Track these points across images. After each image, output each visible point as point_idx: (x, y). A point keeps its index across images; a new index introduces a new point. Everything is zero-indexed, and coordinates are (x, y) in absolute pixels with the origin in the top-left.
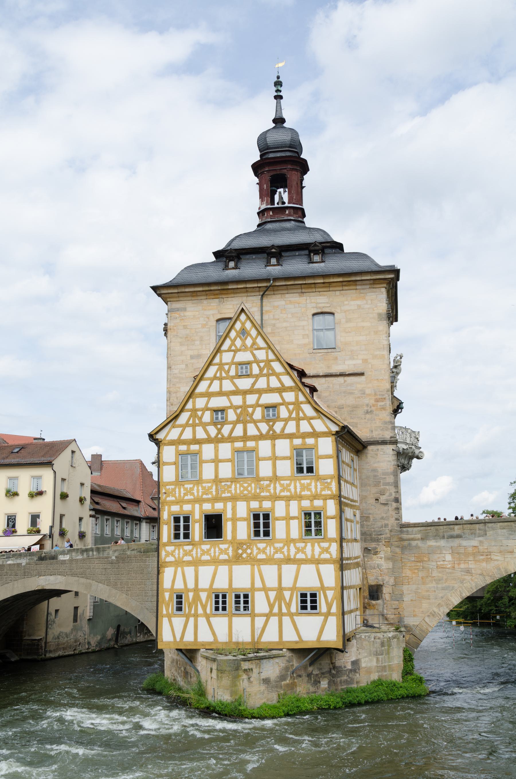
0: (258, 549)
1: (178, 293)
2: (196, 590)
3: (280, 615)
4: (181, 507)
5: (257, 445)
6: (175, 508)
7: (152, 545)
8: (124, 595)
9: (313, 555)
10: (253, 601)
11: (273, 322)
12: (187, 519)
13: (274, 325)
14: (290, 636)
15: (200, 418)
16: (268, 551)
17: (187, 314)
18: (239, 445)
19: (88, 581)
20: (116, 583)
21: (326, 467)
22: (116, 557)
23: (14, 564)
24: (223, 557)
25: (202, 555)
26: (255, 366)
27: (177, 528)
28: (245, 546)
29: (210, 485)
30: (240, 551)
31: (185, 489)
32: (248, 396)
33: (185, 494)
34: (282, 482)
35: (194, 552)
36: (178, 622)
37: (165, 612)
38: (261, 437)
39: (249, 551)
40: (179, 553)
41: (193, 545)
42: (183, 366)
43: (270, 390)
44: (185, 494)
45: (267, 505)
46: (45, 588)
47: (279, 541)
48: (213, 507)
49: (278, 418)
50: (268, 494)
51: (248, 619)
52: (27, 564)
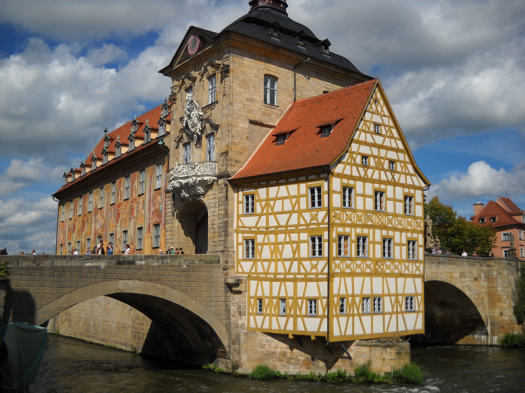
0: (386, 266)
1: (242, 42)
2: (353, 296)
3: (397, 313)
4: (344, 230)
5: (386, 188)
6: (340, 230)
7: (215, 257)
8: (194, 300)
9: (412, 271)
10: (383, 304)
11: (301, 89)
12: (346, 238)
13: (301, 92)
14: (402, 328)
15: (355, 160)
16: (391, 268)
17: (244, 62)
18: (377, 186)
19: (164, 286)
20: (187, 289)
21: (419, 211)
22: (187, 266)
23: (93, 267)
24: (368, 271)
25: (356, 268)
26: (383, 127)
27: (340, 246)
28: (379, 264)
29: (361, 214)
30: (377, 267)
31: (347, 215)
32: (381, 150)
33: (347, 219)
34: (398, 218)
35: (352, 266)
36: (343, 320)
37: (334, 313)
38: (387, 183)
39: (382, 267)
40: (343, 266)
41: (351, 260)
42: (241, 106)
43: (392, 149)
44: (347, 219)
45: (391, 233)
46: (124, 292)
47: (397, 261)
48: (362, 231)
49: (396, 172)
50: (391, 226)
51: (381, 317)
52: (106, 267)
